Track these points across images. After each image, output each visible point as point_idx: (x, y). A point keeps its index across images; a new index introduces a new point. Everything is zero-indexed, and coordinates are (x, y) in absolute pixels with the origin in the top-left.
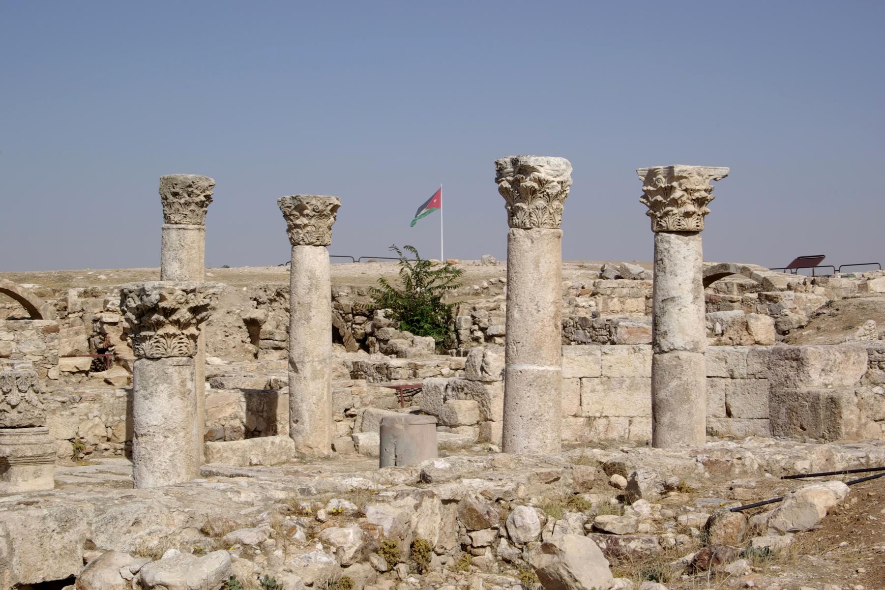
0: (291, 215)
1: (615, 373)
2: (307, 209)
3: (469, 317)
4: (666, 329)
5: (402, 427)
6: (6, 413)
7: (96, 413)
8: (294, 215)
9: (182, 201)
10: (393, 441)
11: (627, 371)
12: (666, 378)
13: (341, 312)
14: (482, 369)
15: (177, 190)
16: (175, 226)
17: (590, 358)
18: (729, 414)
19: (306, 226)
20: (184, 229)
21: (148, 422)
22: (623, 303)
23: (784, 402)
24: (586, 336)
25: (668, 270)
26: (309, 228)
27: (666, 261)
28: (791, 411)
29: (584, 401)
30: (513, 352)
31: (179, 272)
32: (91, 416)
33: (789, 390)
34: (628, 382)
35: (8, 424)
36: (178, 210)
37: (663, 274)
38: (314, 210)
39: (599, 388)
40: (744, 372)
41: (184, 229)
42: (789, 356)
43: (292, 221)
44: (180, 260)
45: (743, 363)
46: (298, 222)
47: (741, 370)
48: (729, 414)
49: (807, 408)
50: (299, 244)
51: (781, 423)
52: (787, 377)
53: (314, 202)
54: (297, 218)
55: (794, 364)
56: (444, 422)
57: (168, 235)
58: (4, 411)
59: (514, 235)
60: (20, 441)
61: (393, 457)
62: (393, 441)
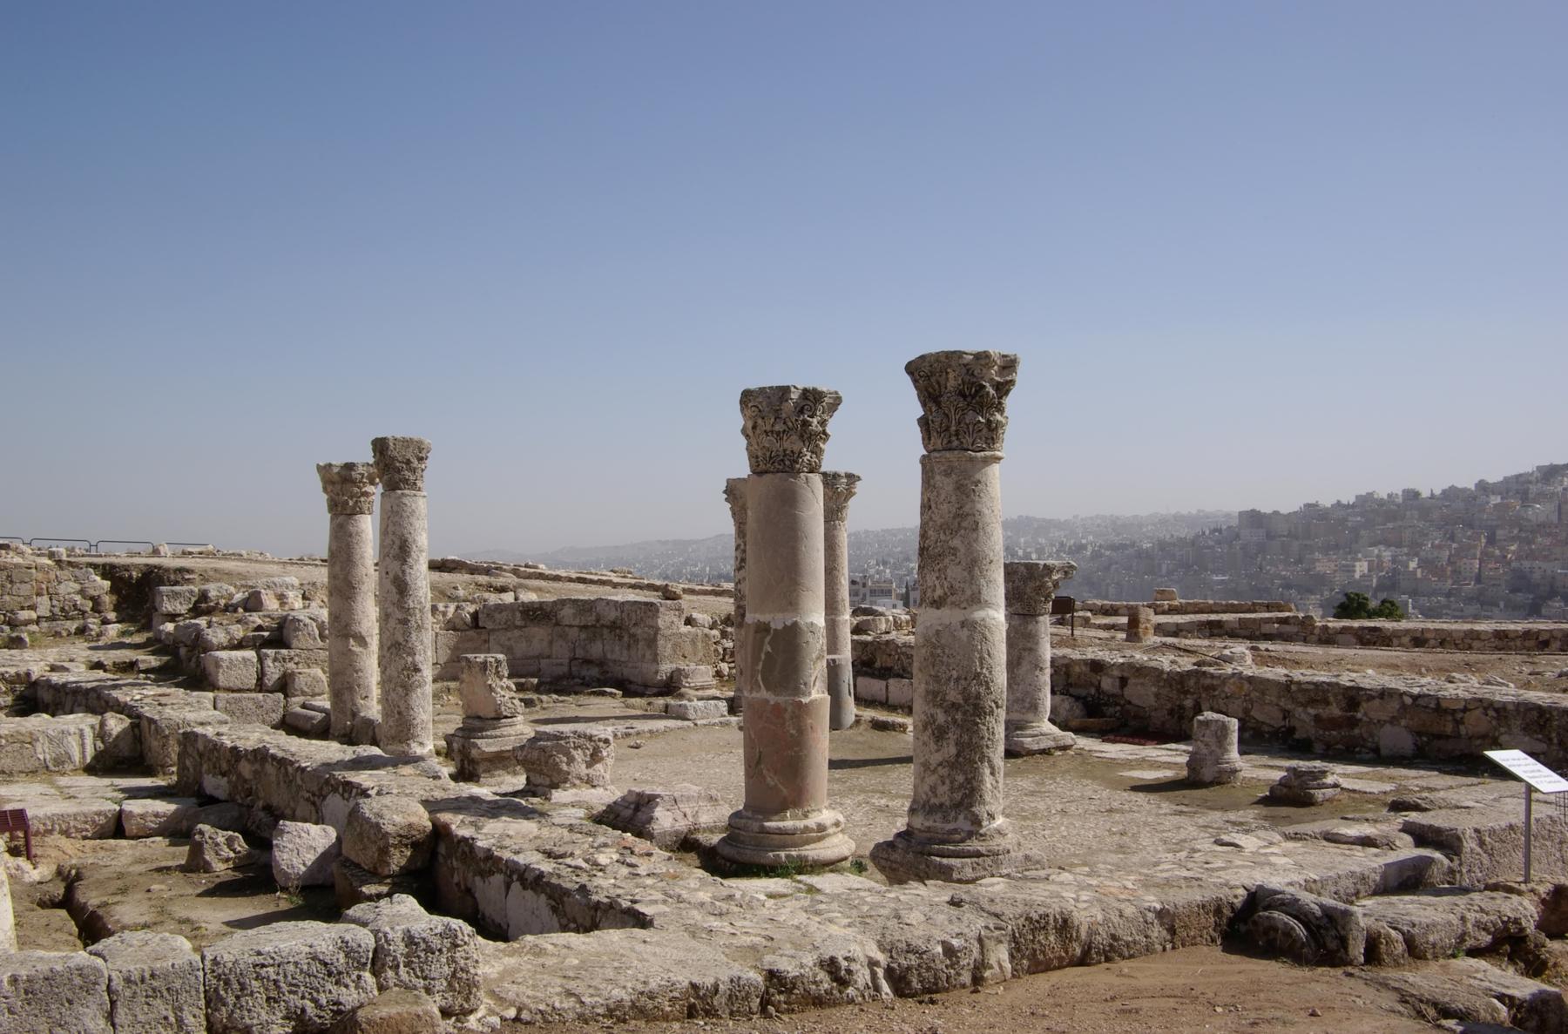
28: (675, 645)
50: (362, 513)
55: (677, 613)
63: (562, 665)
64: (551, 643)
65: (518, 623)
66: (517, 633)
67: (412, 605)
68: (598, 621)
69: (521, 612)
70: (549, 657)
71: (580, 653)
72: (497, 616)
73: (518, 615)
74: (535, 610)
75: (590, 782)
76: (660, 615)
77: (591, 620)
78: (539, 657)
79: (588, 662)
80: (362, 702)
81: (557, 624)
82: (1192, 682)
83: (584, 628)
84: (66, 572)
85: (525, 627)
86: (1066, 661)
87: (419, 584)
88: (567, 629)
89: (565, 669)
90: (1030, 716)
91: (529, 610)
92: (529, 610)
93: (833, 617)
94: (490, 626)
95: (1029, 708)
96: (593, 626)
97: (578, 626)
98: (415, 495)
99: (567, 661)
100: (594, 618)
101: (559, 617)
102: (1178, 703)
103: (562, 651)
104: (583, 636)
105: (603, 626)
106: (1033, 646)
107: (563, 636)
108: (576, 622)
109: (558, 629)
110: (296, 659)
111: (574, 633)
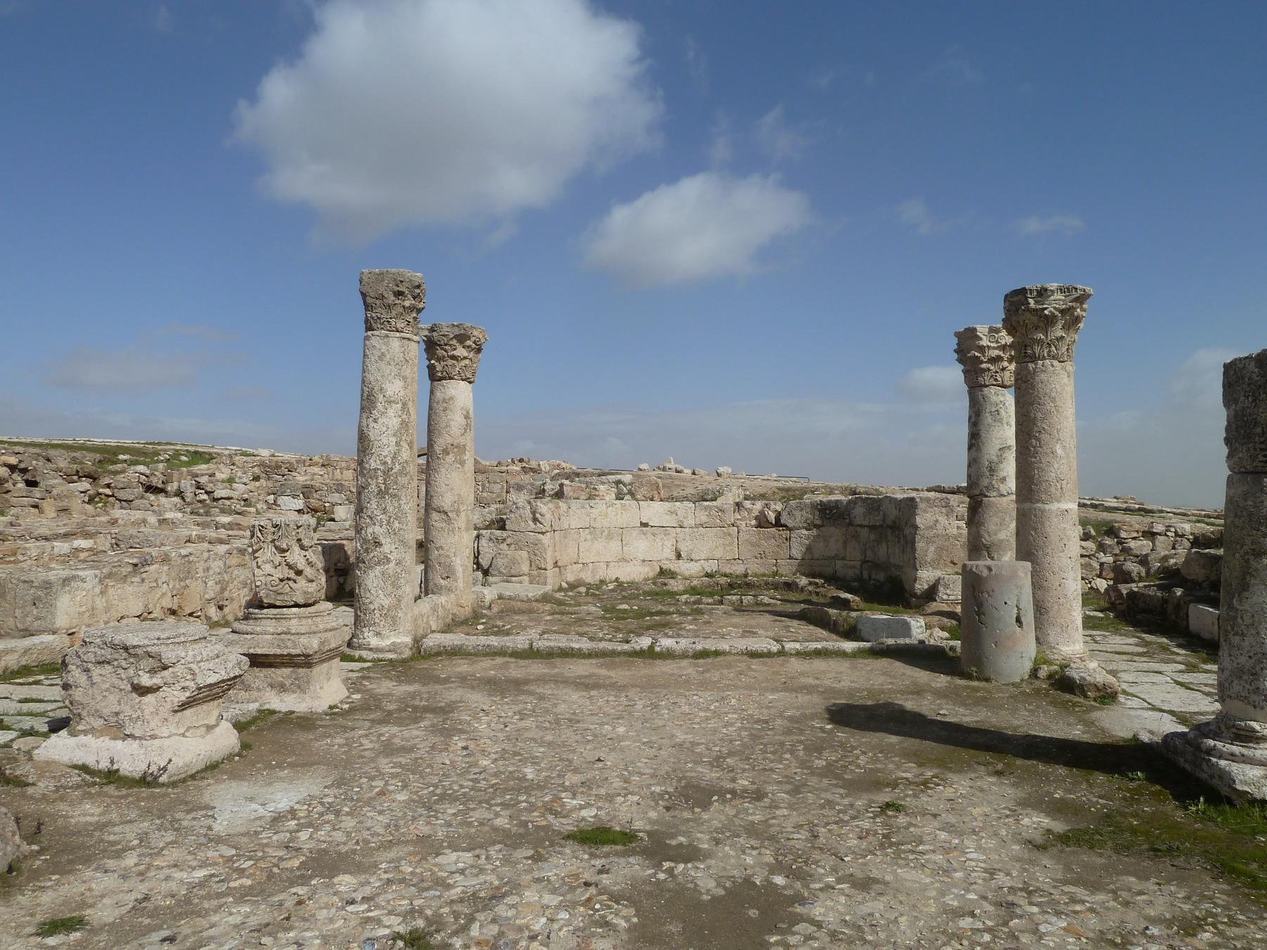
0: (446, 345)
1: (598, 525)
2: (469, 339)
3: (194, 482)
4: (1005, 474)
6: (291, 583)
7: (164, 578)
8: (450, 345)
9: (407, 304)
10: (1016, 592)
11: (606, 523)
12: (1007, 519)
13: (61, 474)
15: (401, 289)
16: (398, 334)
17: (583, 511)
18: (679, 556)
19: (465, 358)
20: (409, 339)
22: (342, 473)
23: (934, 542)
24: (342, 498)
25: (1005, 421)
26: (467, 362)
27: (1002, 411)
28: (940, 550)
29: (581, 550)
30: (1057, 490)
31: (402, 393)
32: (160, 583)
33: (940, 532)
34: (606, 533)
35: (301, 601)
37: (999, 424)
38: (474, 342)
39: (589, 537)
40: (692, 522)
41: (409, 339)
42: (939, 504)
43: (446, 351)
44: (405, 378)
45: (691, 516)
46: (455, 353)
47: (691, 521)
48: (679, 556)
49: (959, 547)
50: (451, 378)
51: (929, 560)
52: (937, 521)
53: (475, 333)
54: (455, 349)
55: (944, 510)
56: (500, 572)
57: (387, 344)
58: (289, 579)
59: (1053, 366)
60: (321, 627)
61: (1015, 611)
62: (1016, 592)
63: (854, 567)
64: (845, 543)
68: (884, 520)
69: (819, 510)
70: (843, 559)
71: (869, 555)
75: (116, 729)
76: (918, 511)
77: (877, 520)
78: (836, 557)
79: (876, 566)
80: (443, 582)
81: (850, 524)
83: (872, 528)
84: (527, 476)
85: (822, 526)
88: (859, 529)
89: (858, 572)
91: (826, 509)
92: (826, 509)
94: (790, 523)
96: (881, 526)
97: (867, 526)
98: (387, 336)
99: (859, 563)
100: (881, 517)
101: (852, 516)
103: (854, 553)
104: (872, 537)
105: (888, 526)
107: (856, 537)
108: (865, 523)
109: (851, 528)
110: (509, 541)
111: (864, 533)
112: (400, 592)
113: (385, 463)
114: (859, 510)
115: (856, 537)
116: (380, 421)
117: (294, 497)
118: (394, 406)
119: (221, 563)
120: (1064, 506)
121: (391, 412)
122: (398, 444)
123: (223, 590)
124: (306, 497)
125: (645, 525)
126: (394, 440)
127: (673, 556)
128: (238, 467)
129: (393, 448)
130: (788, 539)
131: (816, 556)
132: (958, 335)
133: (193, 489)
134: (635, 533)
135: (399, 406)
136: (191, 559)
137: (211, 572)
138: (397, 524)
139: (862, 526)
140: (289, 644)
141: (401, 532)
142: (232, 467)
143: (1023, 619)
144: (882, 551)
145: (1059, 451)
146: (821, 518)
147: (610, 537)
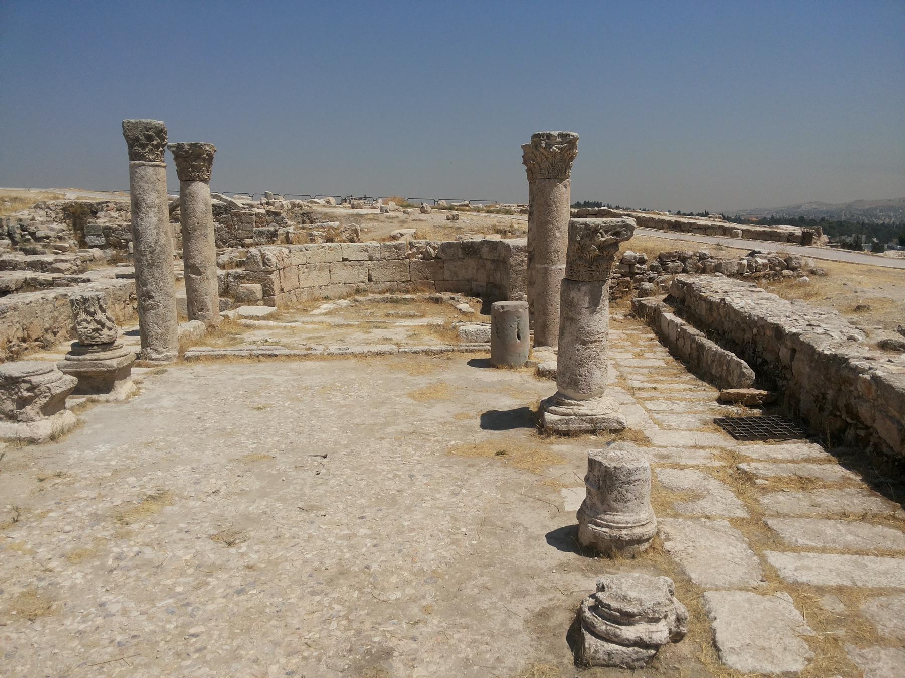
5: (522, 311)
9: (155, 142)
11: (317, 259)
14: (265, 264)
16: (151, 163)
17: (301, 253)
18: (370, 280)
21: (598, 330)
31: (157, 201)
36: (152, 150)
41: (159, 166)
48: (370, 280)
62: (517, 320)
63: (483, 286)
64: (477, 270)
65: (460, 256)
66: (459, 263)
67: (143, 249)
70: (476, 280)
71: (492, 279)
72: (448, 250)
73: (460, 250)
74: (469, 247)
81: (481, 258)
82: (833, 370)
83: (493, 261)
84: (271, 218)
85: (464, 258)
86: (762, 323)
87: (149, 232)
90: (570, 392)
93: (546, 265)
95: (569, 384)
96: (498, 260)
102: (822, 390)
106: (574, 317)
108: (489, 258)
111: (488, 264)
112: (168, 324)
113: (151, 246)
114: (485, 249)
115: (484, 266)
116: (144, 220)
117: (98, 235)
118: (153, 209)
119: (51, 306)
120: (559, 267)
121: (151, 214)
122: (158, 234)
123: (54, 322)
124: (106, 236)
125: (345, 260)
126: (155, 231)
127: (366, 279)
128: (51, 210)
129: (155, 237)
130: (442, 268)
131: (460, 278)
132: (523, 147)
133: (19, 231)
134: (339, 265)
135: (156, 210)
136: (32, 305)
137: (46, 312)
138: (162, 284)
139: (486, 259)
140: (100, 366)
141: (166, 288)
142: (46, 210)
143: (521, 335)
144: (498, 276)
145: (558, 234)
146: (462, 254)
147: (321, 269)
